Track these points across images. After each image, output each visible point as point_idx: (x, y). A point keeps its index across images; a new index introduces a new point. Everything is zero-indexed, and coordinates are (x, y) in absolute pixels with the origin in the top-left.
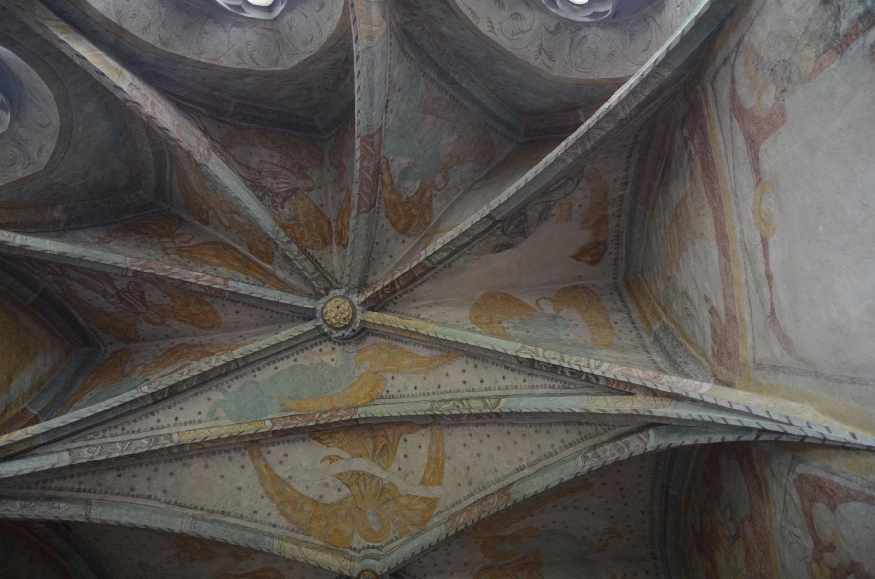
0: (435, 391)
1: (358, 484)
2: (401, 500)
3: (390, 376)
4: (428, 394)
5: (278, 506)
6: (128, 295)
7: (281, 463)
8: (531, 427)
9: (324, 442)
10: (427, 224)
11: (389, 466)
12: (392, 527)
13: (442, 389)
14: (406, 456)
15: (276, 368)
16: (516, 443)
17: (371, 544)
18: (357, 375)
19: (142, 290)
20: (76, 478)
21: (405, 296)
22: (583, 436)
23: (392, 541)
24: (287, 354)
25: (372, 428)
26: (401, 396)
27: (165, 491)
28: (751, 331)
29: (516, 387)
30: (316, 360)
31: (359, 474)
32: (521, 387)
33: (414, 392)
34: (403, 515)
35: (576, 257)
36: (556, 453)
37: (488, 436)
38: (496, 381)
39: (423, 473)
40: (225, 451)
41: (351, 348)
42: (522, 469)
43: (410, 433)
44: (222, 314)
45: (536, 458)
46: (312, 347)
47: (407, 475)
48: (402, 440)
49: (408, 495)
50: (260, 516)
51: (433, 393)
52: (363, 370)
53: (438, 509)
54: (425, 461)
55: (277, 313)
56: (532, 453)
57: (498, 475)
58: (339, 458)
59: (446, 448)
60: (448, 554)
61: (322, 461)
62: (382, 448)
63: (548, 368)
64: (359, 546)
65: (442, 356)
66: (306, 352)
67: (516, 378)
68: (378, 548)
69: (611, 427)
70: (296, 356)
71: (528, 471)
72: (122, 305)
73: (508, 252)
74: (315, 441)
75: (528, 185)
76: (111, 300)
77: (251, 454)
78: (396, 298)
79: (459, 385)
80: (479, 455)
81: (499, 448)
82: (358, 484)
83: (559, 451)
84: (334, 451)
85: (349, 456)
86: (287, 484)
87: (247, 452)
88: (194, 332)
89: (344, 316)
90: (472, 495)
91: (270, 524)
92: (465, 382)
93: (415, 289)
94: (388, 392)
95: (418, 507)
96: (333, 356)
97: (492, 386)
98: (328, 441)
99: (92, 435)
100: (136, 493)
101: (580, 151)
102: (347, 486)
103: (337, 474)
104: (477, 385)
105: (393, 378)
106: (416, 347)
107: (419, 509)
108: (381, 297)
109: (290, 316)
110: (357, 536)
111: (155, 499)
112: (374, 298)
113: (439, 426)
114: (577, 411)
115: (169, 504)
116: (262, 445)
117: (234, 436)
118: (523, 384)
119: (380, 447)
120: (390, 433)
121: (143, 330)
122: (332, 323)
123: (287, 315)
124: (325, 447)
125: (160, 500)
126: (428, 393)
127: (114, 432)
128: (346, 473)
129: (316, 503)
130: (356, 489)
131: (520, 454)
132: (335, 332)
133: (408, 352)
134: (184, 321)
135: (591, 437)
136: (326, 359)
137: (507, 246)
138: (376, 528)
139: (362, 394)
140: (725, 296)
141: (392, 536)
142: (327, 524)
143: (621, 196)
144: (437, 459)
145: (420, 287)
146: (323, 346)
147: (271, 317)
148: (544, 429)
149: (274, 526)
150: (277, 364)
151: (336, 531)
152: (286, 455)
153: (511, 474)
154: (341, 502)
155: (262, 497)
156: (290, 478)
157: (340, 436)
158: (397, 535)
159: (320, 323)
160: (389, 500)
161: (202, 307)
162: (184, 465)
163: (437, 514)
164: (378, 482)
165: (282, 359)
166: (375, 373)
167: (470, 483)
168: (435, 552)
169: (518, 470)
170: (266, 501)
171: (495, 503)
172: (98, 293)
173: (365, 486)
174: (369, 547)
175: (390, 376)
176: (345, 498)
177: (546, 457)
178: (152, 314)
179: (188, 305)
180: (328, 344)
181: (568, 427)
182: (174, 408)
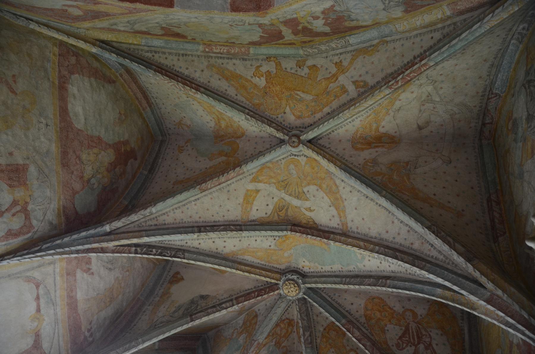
0: (243, 238)
1: (299, 192)
2: (275, 181)
3: (272, 247)
4: (248, 237)
5: (339, 192)
6: (412, 340)
7: (333, 216)
8: (185, 222)
9: (312, 220)
10: (248, 314)
11: (279, 200)
12: (282, 166)
13: (238, 239)
14: (267, 205)
15: (331, 268)
16: (197, 213)
17: (296, 157)
18: (292, 250)
19: (399, 341)
20: (431, 255)
21: (260, 285)
22: (156, 219)
23: (283, 159)
24: (326, 273)
25: (287, 221)
26: (266, 237)
27: (393, 222)
28: (56, 274)
29: (192, 240)
30: (312, 265)
31: (298, 197)
32: (189, 240)
33: (257, 238)
34: (274, 173)
35: (182, 279)
36: (173, 210)
37: (213, 216)
38: (204, 242)
39: (258, 196)
40: (359, 233)
41: (293, 265)
42: (196, 200)
43: (262, 217)
44: (362, 306)
45: (186, 206)
46: (314, 272)
47: (269, 195)
48: (269, 213)
49: (269, 184)
50: (348, 189)
51: (245, 237)
52: (289, 252)
53: (251, 177)
54: (255, 203)
55: (329, 296)
56: (188, 209)
57: (210, 196)
58: (306, 209)
59: (241, 209)
60: (255, 148)
61: (314, 210)
62: (282, 210)
63: (166, 252)
64: (303, 157)
65: (237, 255)
66: (317, 271)
67: (192, 244)
68: (293, 155)
69: (136, 226)
70: (322, 270)
71: (193, 199)
72: (424, 333)
73: (204, 293)
74: (316, 222)
75: (164, 333)
76: (428, 340)
77: (347, 227)
78: (265, 285)
79: (229, 241)
80: (221, 206)
81: (208, 210)
82: (299, 192)
83: (171, 211)
84: (308, 214)
85: (302, 209)
86: (332, 203)
87: (349, 229)
88: (389, 298)
89: (287, 287)
90: (228, 185)
91: (345, 182)
92: (225, 242)
93: (253, 287)
94: (275, 239)
95: (264, 177)
96: (303, 264)
97: (207, 240)
98: (310, 220)
99: (420, 276)
100: (407, 228)
101: (133, 343)
102: (304, 193)
103: (308, 201)
104: (217, 241)
105: (270, 246)
106: (252, 261)
107: (264, 176)
108: (268, 290)
109: (324, 291)
110: (303, 163)
111: (399, 220)
112: (272, 290)
113: (243, 221)
114: (146, 238)
115: (393, 213)
116: (341, 230)
117: (345, 244)
118: (188, 241)
119: (284, 210)
120: (276, 218)
121: (424, 309)
122: (294, 285)
123: (325, 293)
124: (312, 217)
125: (396, 218)
126: (248, 237)
127: (411, 272)
128: (304, 200)
129: (321, 187)
130: (300, 190)
131: (195, 207)
132: (295, 279)
133: (258, 259)
134: (390, 308)
135: (151, 219)
136: (307, 263)
137: (202, 297)
138: (292, 166)
139: (291, 240)
140: (75, 280)
141: (283, 161)
142: (317, 173)
143: (149, 305)
144: (247, 204)
145: (250, 288)
146: (308, 270)
147: (335, 295)
148: (177, 221)
149: (343, 181)
150: (331, 270)
151: (313, 169)
152: (330, 220)
153: (202, 197)
154: (309, 184)
155: (346, 200)
156: (330, 206)
157: (304, 221)
158: (280, 162)
159: (302, 286)
160: (282, 181)
161: (371, 315)
162: (380, 234)
163: (252, 174)
164: (287, 192)
165: (328, 272)
166: (281, 249)
167: (229, 191)
168: (261, 150)
169: (198, 199)
170: (344, 197)
171: (209, 185)
172: (433, 348)
173: (295, 191)
174: (298, 156)
175: (272, 247)
176: (306, 186)
177: (179, 207)
178: (408, 319)
179: (379, 319)
180: (306, 271)
181: (163, 222)
182: (382, 270)
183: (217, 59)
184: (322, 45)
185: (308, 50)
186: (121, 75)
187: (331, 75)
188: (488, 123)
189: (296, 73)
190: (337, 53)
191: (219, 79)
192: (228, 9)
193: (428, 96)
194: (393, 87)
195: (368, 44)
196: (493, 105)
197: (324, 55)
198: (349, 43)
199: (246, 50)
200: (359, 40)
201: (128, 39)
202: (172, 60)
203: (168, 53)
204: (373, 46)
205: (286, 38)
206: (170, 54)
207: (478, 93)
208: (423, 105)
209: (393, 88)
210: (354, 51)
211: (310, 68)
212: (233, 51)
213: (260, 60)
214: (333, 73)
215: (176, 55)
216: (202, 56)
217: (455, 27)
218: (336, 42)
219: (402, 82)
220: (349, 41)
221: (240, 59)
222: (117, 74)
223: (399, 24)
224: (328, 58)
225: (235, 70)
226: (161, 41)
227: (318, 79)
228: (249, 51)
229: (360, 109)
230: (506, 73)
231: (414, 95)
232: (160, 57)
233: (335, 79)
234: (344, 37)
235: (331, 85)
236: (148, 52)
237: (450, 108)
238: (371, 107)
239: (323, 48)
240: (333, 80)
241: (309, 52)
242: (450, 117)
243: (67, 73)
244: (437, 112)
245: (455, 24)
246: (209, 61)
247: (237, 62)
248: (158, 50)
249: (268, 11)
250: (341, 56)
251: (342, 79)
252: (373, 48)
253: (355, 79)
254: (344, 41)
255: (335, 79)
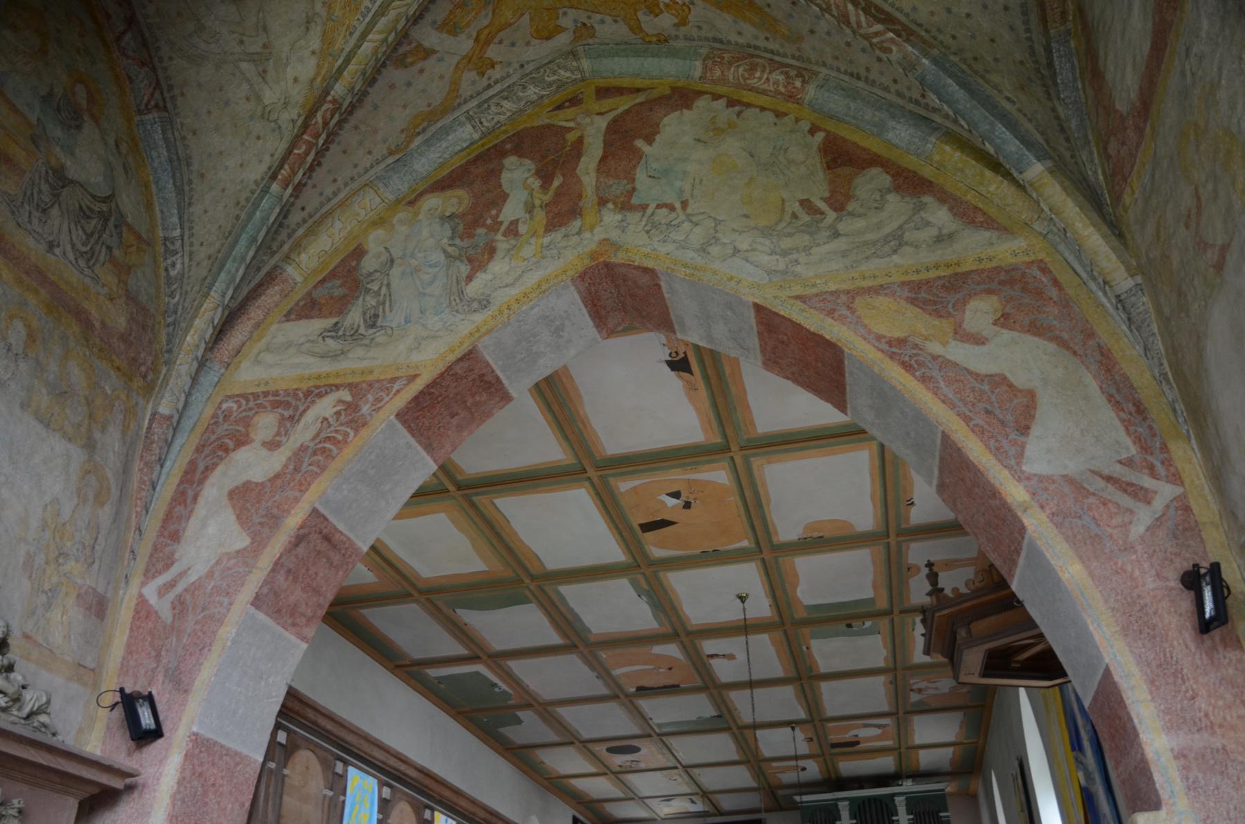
183: (782, 51)
184: (535, 97)
185: (568, 74)
186: (1064, 14)
187: (496, 40)
188: (124, 33)
189: (589, 13)
190: (499, 84)
191: (769, 6)
192: (662, 274)
193: (265, 71)
194: (331, 106)
195: (433, 129)
196: (141, 82)
197: (529, 68)
198: (473, 123)
199: (711, 70)
200: (450, 138)
201: (960, 165)
202: (881, 73)
203: (889, 92)
204: (419, 134)
205: (602, 123)
206: (886, 89)
207: (183, 94)
208: (265, 46)
209: (330, 101)
210: (460, 105)
211: (559, 30)
212: (741, 70)
213: (681, 37)
214: (492, 45)
215: (874, 81)
216: (817, 63)
217: (269, 251)
218: (502, 118)
219: (316, 122)
220: (474, 127)
221: (729, 42)
222: (1070, 25)
223: (374, 207)
224: (517, 66)
225: (735, 22)
226: (890, 135)
227: (527, 17)
228: (705, 67)
229: (383, 20)
230: (156, 165)
231: (290, 73)
232: (909, 89)
233: (483, 37)
234: (486, 136)
235: (486, 22)
236: (933, 108)
237: (212, 46)
238: (367, 20)
239: (532, 92)
240: (486, 32)
241: (566, 69)
242: (203, 22)
243: (1128, 131)
244: (233, 32)
245: (274, 253)
246: (799, 49)
247: (733, 37)
248: (912, 105)
249: (587, 262)
250: (487, 83)
251: (464, 44)
252: (417, 130)
253: (432, 60)
254: (485, 123)
255: (483, 37)
